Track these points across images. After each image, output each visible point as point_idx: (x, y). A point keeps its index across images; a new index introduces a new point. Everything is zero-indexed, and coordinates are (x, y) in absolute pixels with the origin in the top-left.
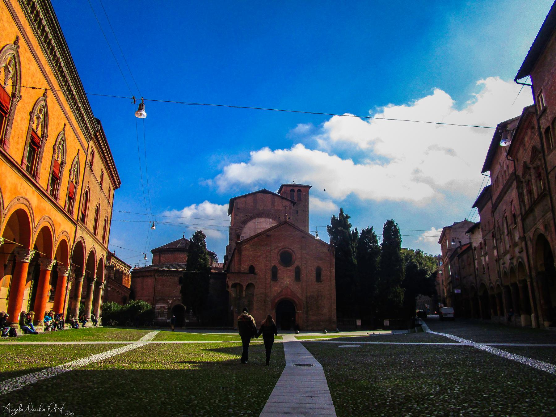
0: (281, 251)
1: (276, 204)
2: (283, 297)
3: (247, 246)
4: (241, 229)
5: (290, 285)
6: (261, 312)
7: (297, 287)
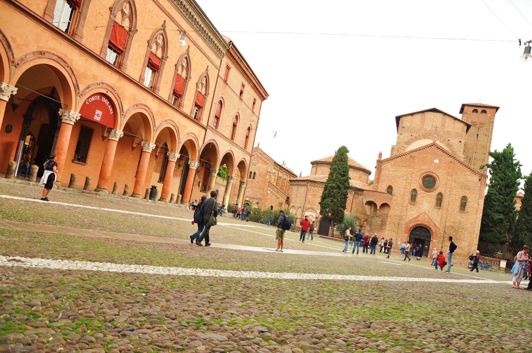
0: (424, 175)
1: (446, 125)
2: (419, 222)
3: (388, 165)
4: (404, 149)
5: (428, 211)
6: (393, 233)
7: (436, 215)
